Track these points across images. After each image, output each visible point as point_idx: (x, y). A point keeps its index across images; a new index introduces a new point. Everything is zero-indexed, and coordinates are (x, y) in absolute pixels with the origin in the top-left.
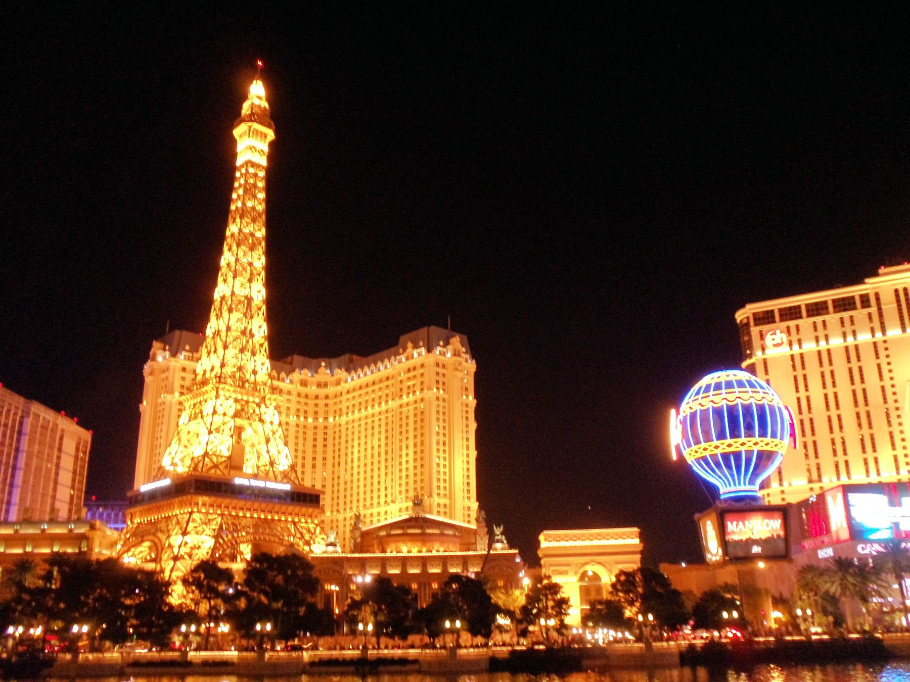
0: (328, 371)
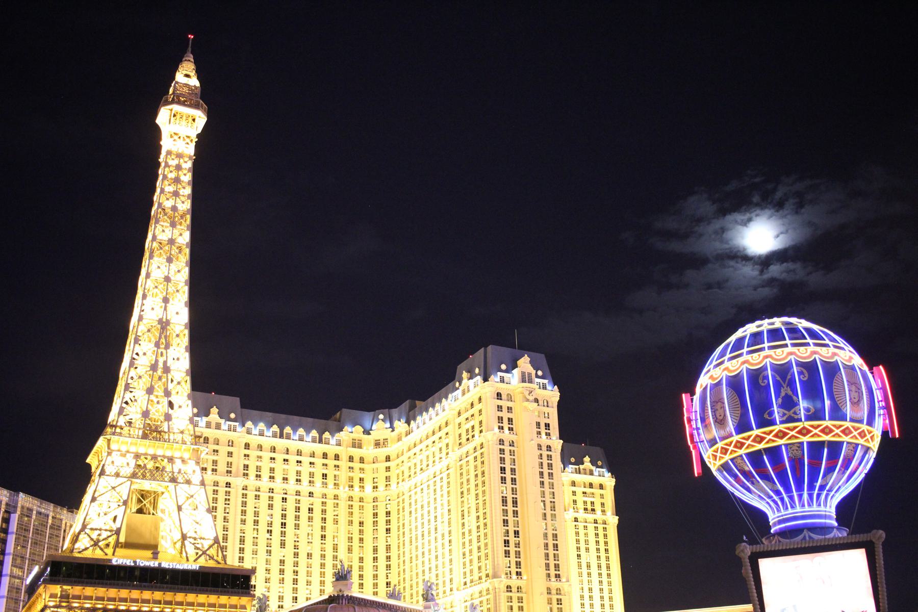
0: (388, 425)
